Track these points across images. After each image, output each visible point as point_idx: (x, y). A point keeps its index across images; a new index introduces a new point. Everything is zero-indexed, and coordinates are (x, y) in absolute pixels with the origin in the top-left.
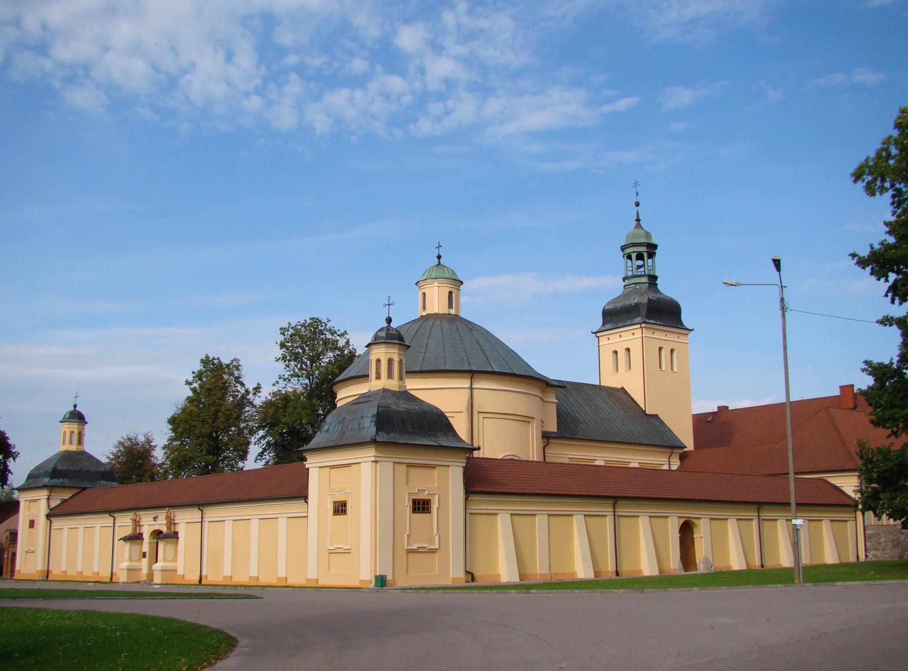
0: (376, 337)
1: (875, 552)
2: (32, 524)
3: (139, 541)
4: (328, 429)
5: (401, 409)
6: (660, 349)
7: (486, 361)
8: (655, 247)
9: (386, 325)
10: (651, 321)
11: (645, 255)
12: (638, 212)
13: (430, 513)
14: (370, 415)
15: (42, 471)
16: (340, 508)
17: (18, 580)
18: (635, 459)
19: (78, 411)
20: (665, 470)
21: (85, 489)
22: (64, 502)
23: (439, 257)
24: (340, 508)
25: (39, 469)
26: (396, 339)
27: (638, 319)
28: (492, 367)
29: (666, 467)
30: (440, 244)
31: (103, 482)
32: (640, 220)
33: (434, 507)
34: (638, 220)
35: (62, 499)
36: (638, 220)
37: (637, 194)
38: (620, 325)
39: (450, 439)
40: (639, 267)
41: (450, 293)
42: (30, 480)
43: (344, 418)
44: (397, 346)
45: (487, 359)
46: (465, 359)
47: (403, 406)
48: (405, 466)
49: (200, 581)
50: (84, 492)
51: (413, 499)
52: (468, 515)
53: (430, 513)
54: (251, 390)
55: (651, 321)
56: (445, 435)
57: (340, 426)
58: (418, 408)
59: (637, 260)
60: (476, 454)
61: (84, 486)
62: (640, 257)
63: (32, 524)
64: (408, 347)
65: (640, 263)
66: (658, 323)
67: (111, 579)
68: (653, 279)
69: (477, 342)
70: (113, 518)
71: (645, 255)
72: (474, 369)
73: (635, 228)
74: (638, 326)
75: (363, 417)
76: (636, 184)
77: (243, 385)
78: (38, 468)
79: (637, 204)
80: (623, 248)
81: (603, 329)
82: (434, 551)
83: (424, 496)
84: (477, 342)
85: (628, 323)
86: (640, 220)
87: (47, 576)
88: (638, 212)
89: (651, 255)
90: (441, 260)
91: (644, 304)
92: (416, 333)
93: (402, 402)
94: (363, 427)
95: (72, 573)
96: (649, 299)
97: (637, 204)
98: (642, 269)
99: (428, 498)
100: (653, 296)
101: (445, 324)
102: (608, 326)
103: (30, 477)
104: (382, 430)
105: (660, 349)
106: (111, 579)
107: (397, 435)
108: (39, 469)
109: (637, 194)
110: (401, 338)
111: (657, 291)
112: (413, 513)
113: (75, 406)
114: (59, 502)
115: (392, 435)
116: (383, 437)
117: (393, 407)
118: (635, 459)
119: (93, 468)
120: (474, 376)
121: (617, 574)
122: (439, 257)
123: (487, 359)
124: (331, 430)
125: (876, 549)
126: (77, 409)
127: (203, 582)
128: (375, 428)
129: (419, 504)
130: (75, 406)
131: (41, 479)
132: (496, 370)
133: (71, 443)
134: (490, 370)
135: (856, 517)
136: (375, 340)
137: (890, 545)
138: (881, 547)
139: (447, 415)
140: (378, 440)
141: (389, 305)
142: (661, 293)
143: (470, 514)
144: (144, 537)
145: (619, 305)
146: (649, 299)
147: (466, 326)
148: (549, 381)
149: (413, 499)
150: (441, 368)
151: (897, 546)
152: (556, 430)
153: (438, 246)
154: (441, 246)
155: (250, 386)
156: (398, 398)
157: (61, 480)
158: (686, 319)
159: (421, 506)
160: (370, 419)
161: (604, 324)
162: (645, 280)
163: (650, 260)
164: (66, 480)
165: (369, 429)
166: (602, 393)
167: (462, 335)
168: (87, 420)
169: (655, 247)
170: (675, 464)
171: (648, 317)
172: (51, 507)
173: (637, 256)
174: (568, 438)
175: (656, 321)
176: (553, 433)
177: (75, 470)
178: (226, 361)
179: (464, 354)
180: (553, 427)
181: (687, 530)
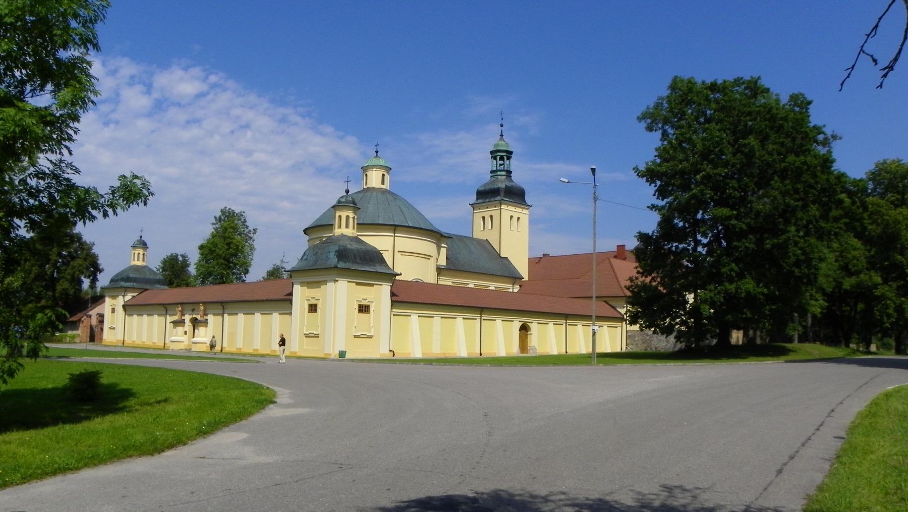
0: (339, 202)
1: (631, 346)
2: (113, 310)
3: (183, 324)
4: (306, 259)
5: (353, 248)
6: (511, 217)
7: (404, 219)
8: (511, 153)
9: (345, 194)
10: (506, 199)
11: (505, 157)
12: (502, 131)
13: (369, 313)
14: (334, 250)
15: (120, 277)
16: (313, 308)
17: (105, 346)
18: (492, 286)
19: (143, 241)
20: (510, 292)
21: (146, 290)
22: (133, 297)
24: (313, 308)
25: (118, 276)
26: (351, 204)
27: (498, 197)
28: (408, 223)
29: (511, 290)
30: (378, 144)
31: (159, 286)
33: (372, 309)
34: (502, 135)
36: (502, 135)
37: (502, 119)
38: (487, 200)
39: (383, 267)
40: (501, 165)
41: (383, 175)
42: (112, 283)
43: (317, 252)
44: (352, 208)
45: (405, 218)
46: (391, 217)
47: (354, 246)
48: (355, 284)
49: (221, 350)
50: (147, 292)
51: (359, 305)
52: (392, 315)
53: (369, 313)
54: (252, 230)
55: (506, 199)
56: (380, 265)
57: (315, 257)
58: (363, 248)
59: (500, 160)
60: (398, 278)
62: (502, 158)
63: (113, 310)
64: (360, 209)
65: (502, 162)
66: (511, 200)
67: (164, 347)
68: (509, 173)
69: (399, 207)
71: (505, 157)
72: (397, 224)
73: (500, 140)
74: (498, 202)
75: (329, 252)
76: (502, 113)
77: (247, 227)
78: (117, 275)
79: (502, 126)
80: (492, 153)
81: (476, 202)
82: (371, 337)
83: (365, 303)
84: (399, 207)
85: (493, 199)
87: (123, 343)
88: (502, 131)
89: (509, 158)
91: (503, 188)
92: (360, 199)
93: (354, 243)
94: (329, 258)
95: (138, 342)
96: (506, 185)
97: (502, 126)
98: (503, 166)
99: (368, 304)
100: (509, 184)
101: (380, 196)
102: (480, 201)
103: (112, 281)
104: (341, 261)
105: (511, 217)
106: (164, 347)
107: (351, 265)
108: (118, 276)
109: (502, 119)
110: (354, 203)
111: (512, 181)
112: (359, 313)
113: (141, 237)
114: (130, 297)
115: (347, 264)
116: (341, 265)
117: (349, 246)
118: (492, 286)
119: (152, 277)
120: (397, 228)
121: (481, 354)
122: (377, 152)
123: (405, 218)
124: (308, 260)
125: (632, 345)
126: (142, 239)
127: (223, 351)
128: (337, 259)
129: (362, 308)
130: (141, 237)
132: (411, 225)
134: (407, 225)
135: (622, 325)
136: (338, 203)
137: (640, 342)
138: (635, 343)
139: (381, 252)
140: (339, 267)
142: (514, 182)
144: (185, 321)
145: (488, 187)
146: (506, 185)
147: (393, 196)
148: (442, 233)
149: (359, 305)
150: (376, 222)
151: (644, 343)
152: (445, 264)
155: (251, 228)
156: (352, 241)
157: (132, 284)
158: (528, 199)
159: (364, 309)
160: (334, 253)
161: (477, 199)
162: (504, 173)
163: (508, 161)
164: (135, 284)
165: (333, 260)
166: (475, 242)
167: (390, 202)
168: (148, 246)
169: (511, 153)
170: (516, 289)
171: (505, 196)
172: (125, 301)
173: (500, 158)
174: (452, 269)
175: (510, 199)
176: (443, 266)
177: (140, 278)
178: (237, 211)
179: (391, 215)
180: (443, 261)
181: (524, 328)
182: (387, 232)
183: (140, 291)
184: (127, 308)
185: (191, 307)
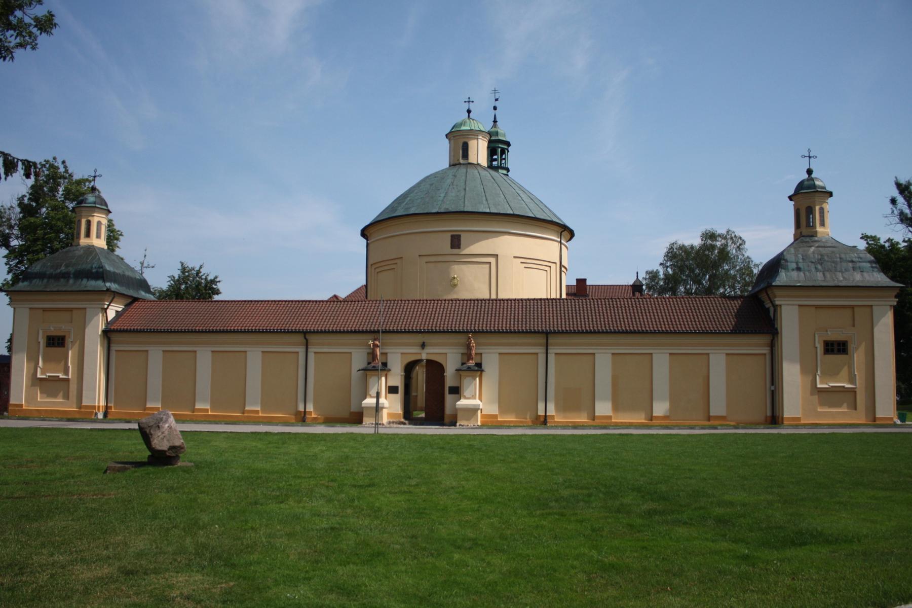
9: (806, 176)
11: (506, 151)
12: (495, 115)
23: (469, 111)
30: (471, 100)
31: (143, 293)
32: (497, 122)
34: (495, 121)
35: (117, 312)
36: (495, 121)
50: (136, 304)
61: (135, 295)
70: (305, 341)
79: (495, 108)
86: (497, 122)
88: (495, 115)
90: (471, 114)
97: (495, 108)
122: (469, 111)
131: (71, 281)
133: (98, 236)
141: (810, 157)
143: (116, 351)
153: (467, 100)
154: (473, 102)
173: (501, 150)
182: (551, 235)
183: (129, 301)
184: (114, 337)
185: (420, 338)
